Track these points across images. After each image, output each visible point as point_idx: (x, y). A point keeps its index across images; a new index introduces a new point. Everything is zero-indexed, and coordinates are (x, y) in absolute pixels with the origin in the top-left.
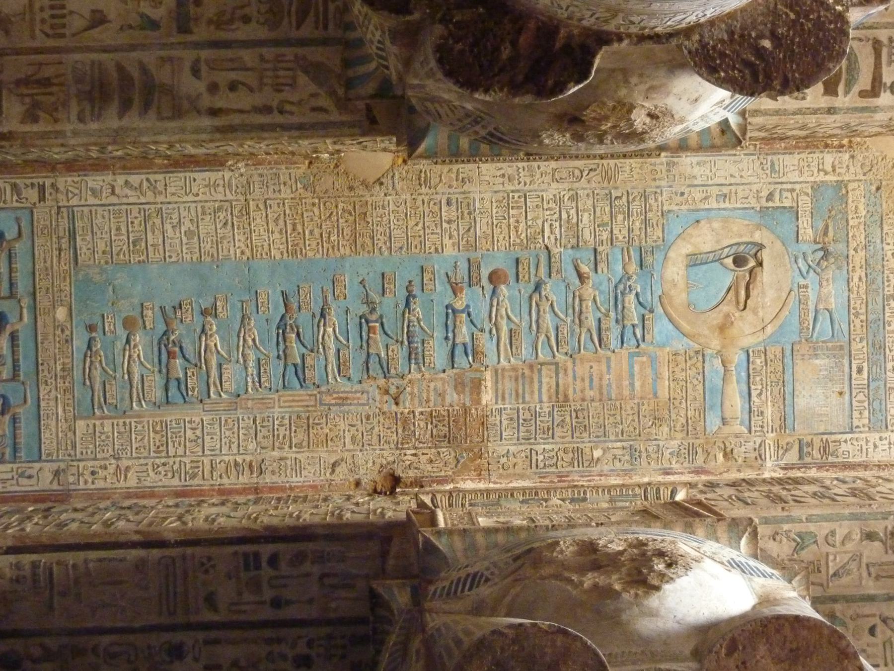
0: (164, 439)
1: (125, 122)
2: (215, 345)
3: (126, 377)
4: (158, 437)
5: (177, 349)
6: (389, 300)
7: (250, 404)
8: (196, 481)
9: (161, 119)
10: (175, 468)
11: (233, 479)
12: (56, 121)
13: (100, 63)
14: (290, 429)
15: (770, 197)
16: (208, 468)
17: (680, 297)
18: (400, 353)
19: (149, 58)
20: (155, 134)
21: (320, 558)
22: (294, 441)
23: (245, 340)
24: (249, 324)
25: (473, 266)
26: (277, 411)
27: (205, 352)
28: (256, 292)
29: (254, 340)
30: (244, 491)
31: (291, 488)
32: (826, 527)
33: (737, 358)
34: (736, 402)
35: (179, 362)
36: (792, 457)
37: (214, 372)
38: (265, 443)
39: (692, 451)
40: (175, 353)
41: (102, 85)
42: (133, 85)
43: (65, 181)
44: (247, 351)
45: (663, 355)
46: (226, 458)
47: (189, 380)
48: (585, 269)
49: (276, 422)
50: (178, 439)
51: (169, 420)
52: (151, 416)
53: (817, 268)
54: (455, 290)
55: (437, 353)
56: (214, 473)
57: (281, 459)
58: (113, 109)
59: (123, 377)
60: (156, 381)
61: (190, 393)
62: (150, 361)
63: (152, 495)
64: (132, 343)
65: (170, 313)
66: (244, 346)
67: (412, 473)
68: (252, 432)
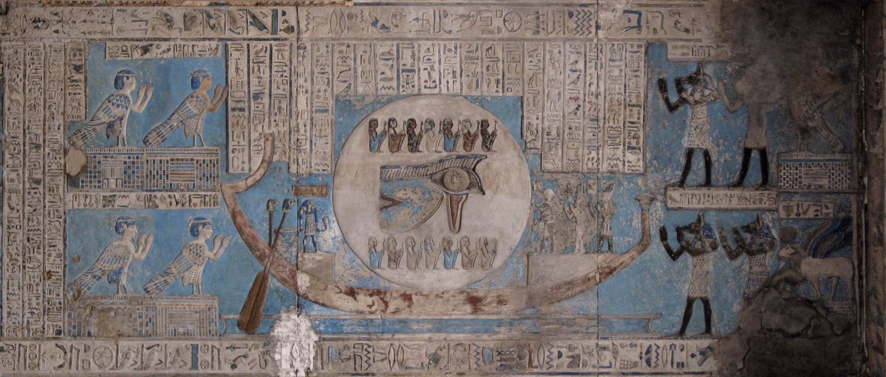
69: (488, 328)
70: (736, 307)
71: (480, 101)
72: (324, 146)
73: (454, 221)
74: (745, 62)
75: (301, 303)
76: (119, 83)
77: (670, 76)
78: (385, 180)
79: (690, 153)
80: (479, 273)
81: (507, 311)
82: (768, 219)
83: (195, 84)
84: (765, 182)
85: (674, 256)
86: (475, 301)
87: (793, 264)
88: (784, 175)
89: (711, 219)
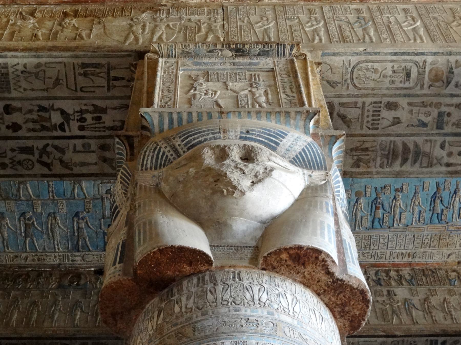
0: (369, 243)
2: (400, 204)
3: (354, 216)
4: (366, 242)
5: (380, 206)
7: (413, 229)
8: (382, 260)
9: (421, 167)
10: (372, 254)
11: (400, 259)
12: (369, 167)
13: (394, 142)
14: (431, 240)
16: (388, 255)
19: (420, 140)
20: (417, 174)
22: (432, 245)
23: (414, 203)
24: (418, 196)
26: (425, 233)
27: (394, 207)
28: (424, 182)
29: (419, 203)
31: (427, 264)
37: (397, 216)
38: (417, 245)
40: (379, 207)
41: (394, 152)
42: (410, 152)
44: (415, 207)
46: (398, 251)
47: (385, 219)
49: (424, 237)
50: (375, 243)
51: (372, 235)
52: (364, 233)
56: (391, 257)
57: (424, 252)
59: (352, 217)
61: (384, 224)
62: (367, 210)
64: (359, 203)
65: (379, 189)
66: (413, 205)
68: (412, 241)
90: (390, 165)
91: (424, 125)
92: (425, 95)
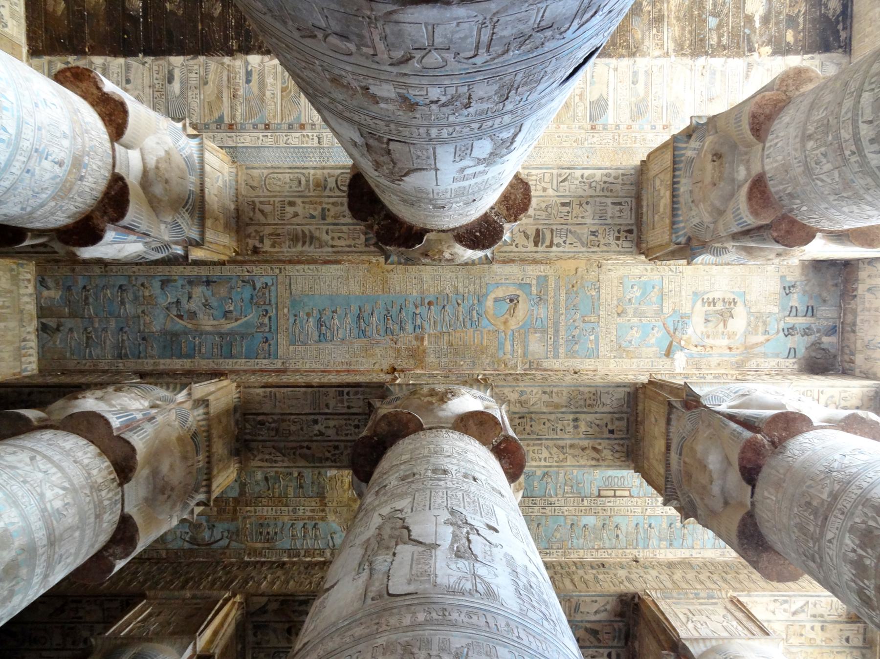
1: (304, 249)
6: (394, 309)
15: (522, 280)
17: (491, 312)
18: (396, 327)
19: (312, 228)
21: (363, 393)
25: (422, 299)
26: (356, 346)
30: (344, 371)
32: (530, 389)
33: (509, 333)
34: (508, 348)
35: (324, 328)
36: (527, 366)
39: (493, 363)
43: (288, 267)
45: (485, 331)
48: (459, 301)
53: (537, 304)
54: (416, 307)
55: (409, 327)
58: (300, 244)
60: (316, 334)
63: (314, 371)
67: (400, 368)
69: (734, 356)
70: (803, 350)
71: (733, 292)
72: (689, 305)
73: (725, 326)
74: (808, 281)
75: (682, 349)
76: (632, 287)
77: (787, 285)
78: (706, 315)
79: (792, 307)
80: (732, 341)
81: (739, 352)
82: (813, 326)
83: (653, 287)
84: (813, 315)
85: (786, 336)
86: (730, 348)
87: (820, 338)
88: (818, 314)
89: (797, 326)
90: (295, 246)
91: (313, 217)
92: (312, 196)
